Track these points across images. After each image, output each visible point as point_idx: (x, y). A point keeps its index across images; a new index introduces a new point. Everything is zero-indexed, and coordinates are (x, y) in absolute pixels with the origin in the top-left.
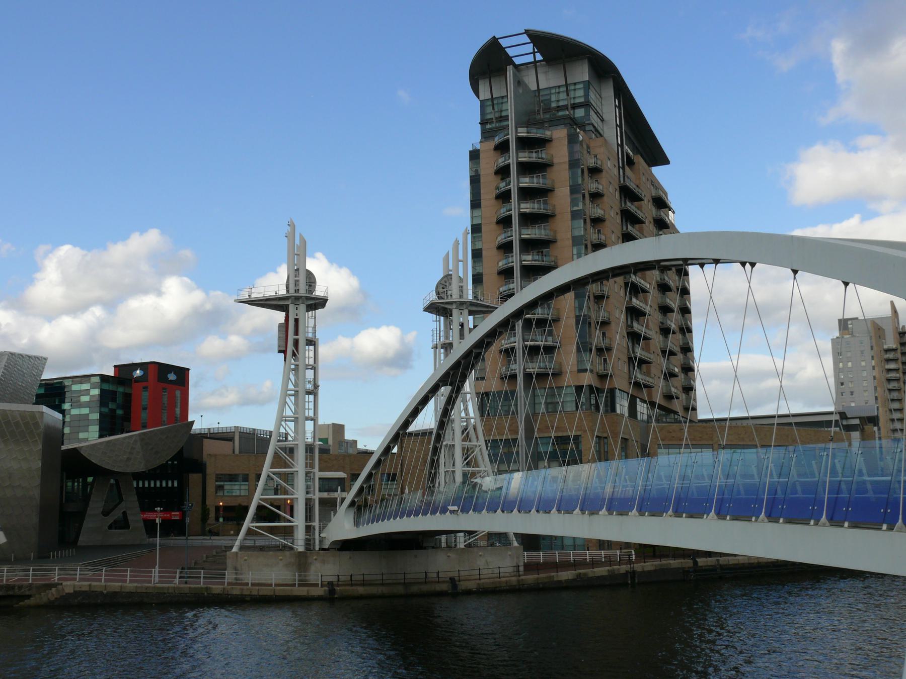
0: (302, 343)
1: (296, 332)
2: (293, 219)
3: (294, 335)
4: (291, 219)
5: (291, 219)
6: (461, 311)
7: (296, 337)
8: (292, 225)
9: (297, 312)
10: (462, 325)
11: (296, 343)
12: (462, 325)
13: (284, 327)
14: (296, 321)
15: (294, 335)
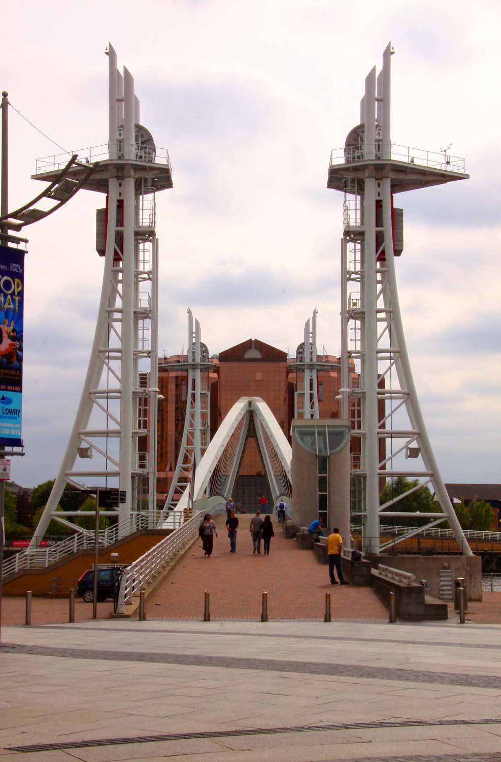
0: (129, 239)
1: (120, 222)
2: (111, 43)
3: (117, 226)
4: (110, 46)
5: (110, 46)
6: (379, 181)
7: (120, 229)
8: (111, 53)
9: (120, 190)
10: (379, 205)
11: (120, 239)
12: (379, 205)
13: (102, 215)
14: (120, 205)
15: (117, 226)
